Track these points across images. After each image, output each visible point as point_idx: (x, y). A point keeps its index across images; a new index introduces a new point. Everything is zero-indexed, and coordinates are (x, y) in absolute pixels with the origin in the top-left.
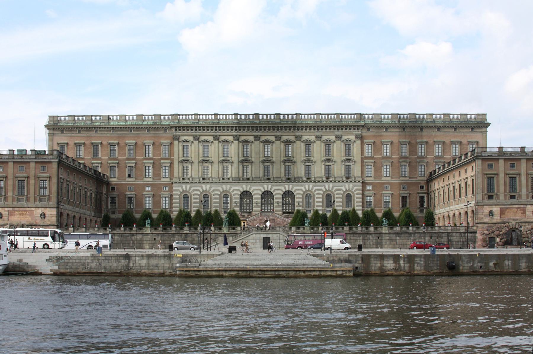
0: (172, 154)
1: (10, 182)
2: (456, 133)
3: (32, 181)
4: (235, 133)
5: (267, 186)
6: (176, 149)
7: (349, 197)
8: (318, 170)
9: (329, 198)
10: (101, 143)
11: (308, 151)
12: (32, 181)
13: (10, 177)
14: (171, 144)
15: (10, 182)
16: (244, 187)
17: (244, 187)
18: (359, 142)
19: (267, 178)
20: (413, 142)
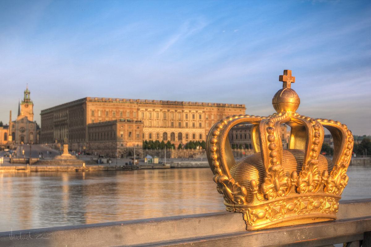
0: (138, 116)
1: (126, 133)
2: (235, 112)
3: (134, 132)
4: (161, 108)
5: (173, 130)
6: (139, 114)
7: (201, 136)
8: (190, 124)
9: (194, 136)
10: (109, 110)
11: (187, 117)
12: (134, 132)
13: (126, 130)
14: (137, 112)
15: (126, 133)
16: (164, 130)
17: (164, 130)
18: (204, 114)
19: (172, 126)
20: (222, 114)
